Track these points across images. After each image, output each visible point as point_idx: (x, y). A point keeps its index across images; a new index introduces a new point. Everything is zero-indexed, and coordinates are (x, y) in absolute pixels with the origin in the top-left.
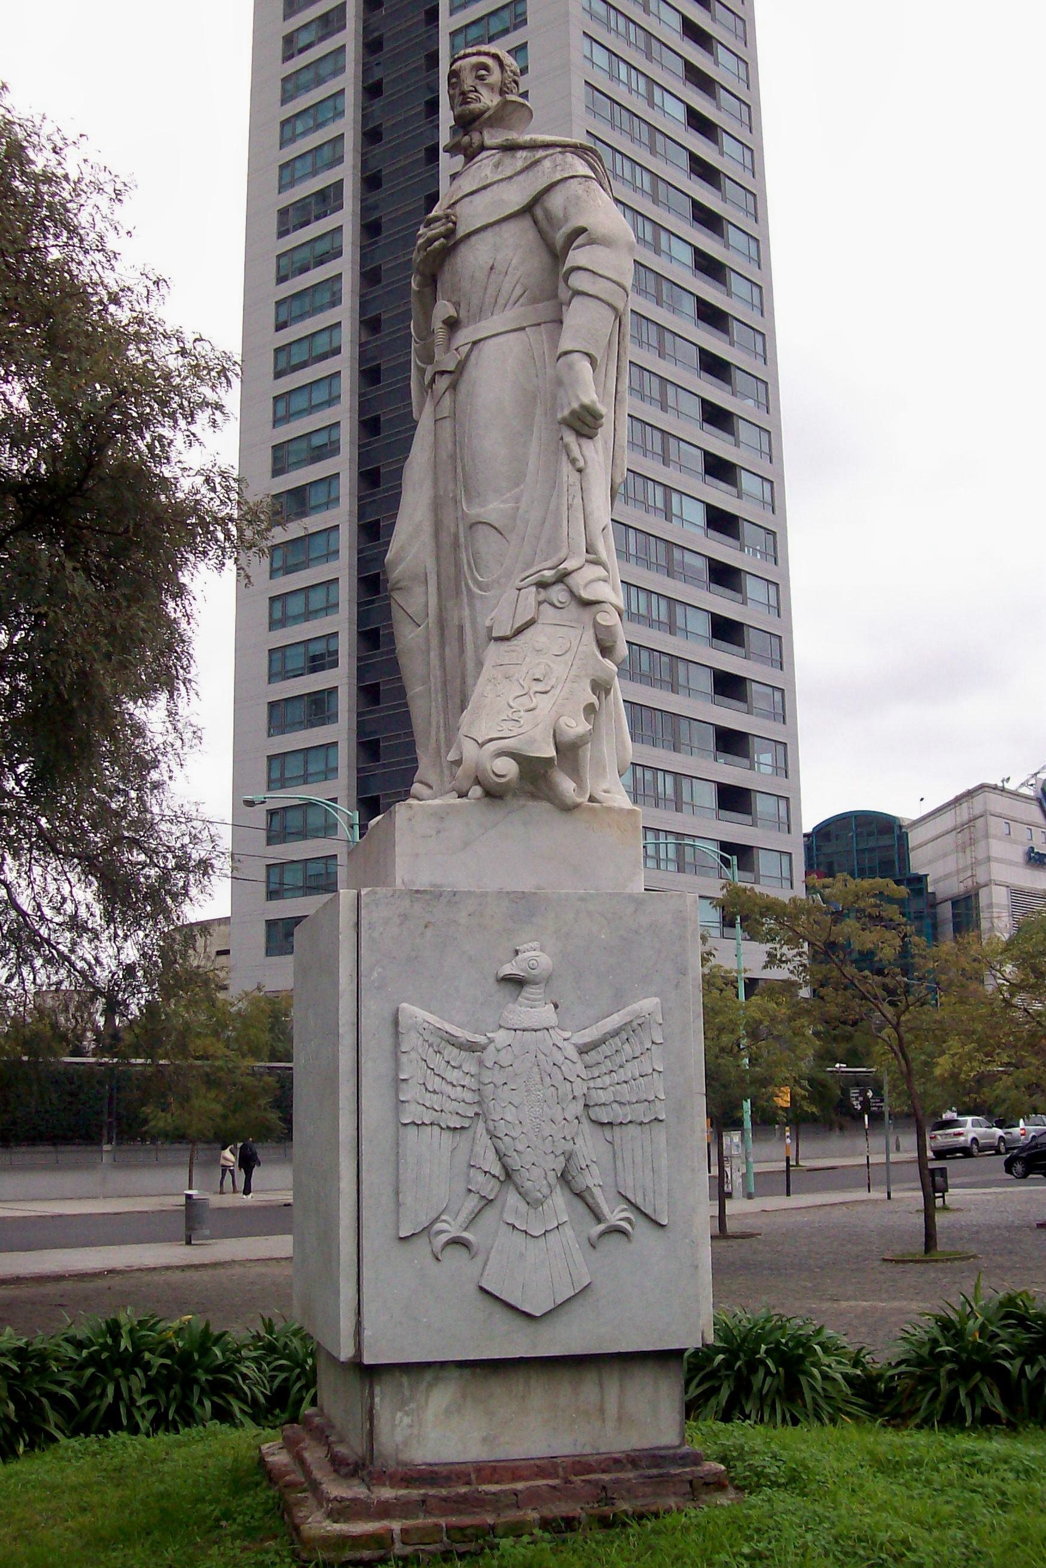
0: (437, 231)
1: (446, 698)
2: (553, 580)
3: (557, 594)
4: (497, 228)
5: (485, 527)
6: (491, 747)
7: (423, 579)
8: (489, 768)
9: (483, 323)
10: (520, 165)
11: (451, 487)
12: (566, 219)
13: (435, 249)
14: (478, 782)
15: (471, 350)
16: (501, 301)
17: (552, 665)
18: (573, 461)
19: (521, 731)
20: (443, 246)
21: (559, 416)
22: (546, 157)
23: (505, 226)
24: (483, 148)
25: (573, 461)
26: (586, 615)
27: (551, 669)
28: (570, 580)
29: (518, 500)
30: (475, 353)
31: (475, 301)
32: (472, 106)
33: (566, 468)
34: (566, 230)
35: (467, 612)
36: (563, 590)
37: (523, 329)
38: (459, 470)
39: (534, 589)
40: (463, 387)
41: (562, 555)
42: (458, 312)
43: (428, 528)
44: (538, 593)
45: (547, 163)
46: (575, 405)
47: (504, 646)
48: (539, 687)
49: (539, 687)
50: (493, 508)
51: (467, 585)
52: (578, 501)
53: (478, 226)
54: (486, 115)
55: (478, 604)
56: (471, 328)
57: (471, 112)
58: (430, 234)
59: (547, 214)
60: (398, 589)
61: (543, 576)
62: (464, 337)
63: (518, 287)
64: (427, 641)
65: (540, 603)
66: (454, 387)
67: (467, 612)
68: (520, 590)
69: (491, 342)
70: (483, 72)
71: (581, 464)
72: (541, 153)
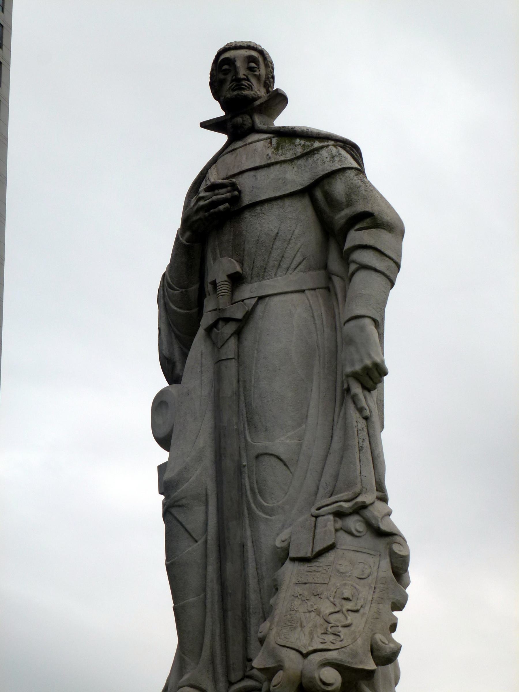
0: (224, 196)
1: (224, 610)
2: (351, 511)
3: (354, 523)
4: (280, 203)
5: (274, 460)
6: (316, 658)
7: (204, 499)
8: (317, 676)
9: (266, 282)
10: (299, 151)
11: (235, 420)
12: (349, 204)
13: (220, 211)
15: (257, 304)
16: (284, 265)
17: (358, 587)
18: (361, 410)
19: (343, 644)
20: (227, 210)
21: (349, 370)
22: (322, 148)
23: (287, 202)
24: (253, 130)
25: (361, 410)
26: (381, 544)
27: (357, 590)
28: (367, 513)
29: (301, 438)
30: (260, 308)
31: (259, 262)
32: (246, 92)
33: (354, 416)
34: (346, 213)
35: (249, 533)
36: (360, 521)
37: (303, 291)
38: (242, 405)
39: (331, 517)
41: (357, 489)
42: (242, 268)
43: (209, 456)
44: (335, 521)
45: (324, 153)
46: (368, 362)
47: (304, 567)
48: (350, 605)
49: (350, 605)
50: (281, 443)
51: (249, 509)
52: (366, 444)
53: (263, 198)
54: (258, 102)
55: (262, 526)
56: (256, 285)
57: (246, 97)
58: (214, 198)
59: (329, 197)
60: (180, 506)
61: (341, 506)
62: (248, 291)
63: (298, 255)
64: (206, 555)
65: (337, 530)
66: (238, 333)
67: (249, 533)
68: (317, 517)
70: (253, 65)
71: (367, 413)
72: (317, 144)
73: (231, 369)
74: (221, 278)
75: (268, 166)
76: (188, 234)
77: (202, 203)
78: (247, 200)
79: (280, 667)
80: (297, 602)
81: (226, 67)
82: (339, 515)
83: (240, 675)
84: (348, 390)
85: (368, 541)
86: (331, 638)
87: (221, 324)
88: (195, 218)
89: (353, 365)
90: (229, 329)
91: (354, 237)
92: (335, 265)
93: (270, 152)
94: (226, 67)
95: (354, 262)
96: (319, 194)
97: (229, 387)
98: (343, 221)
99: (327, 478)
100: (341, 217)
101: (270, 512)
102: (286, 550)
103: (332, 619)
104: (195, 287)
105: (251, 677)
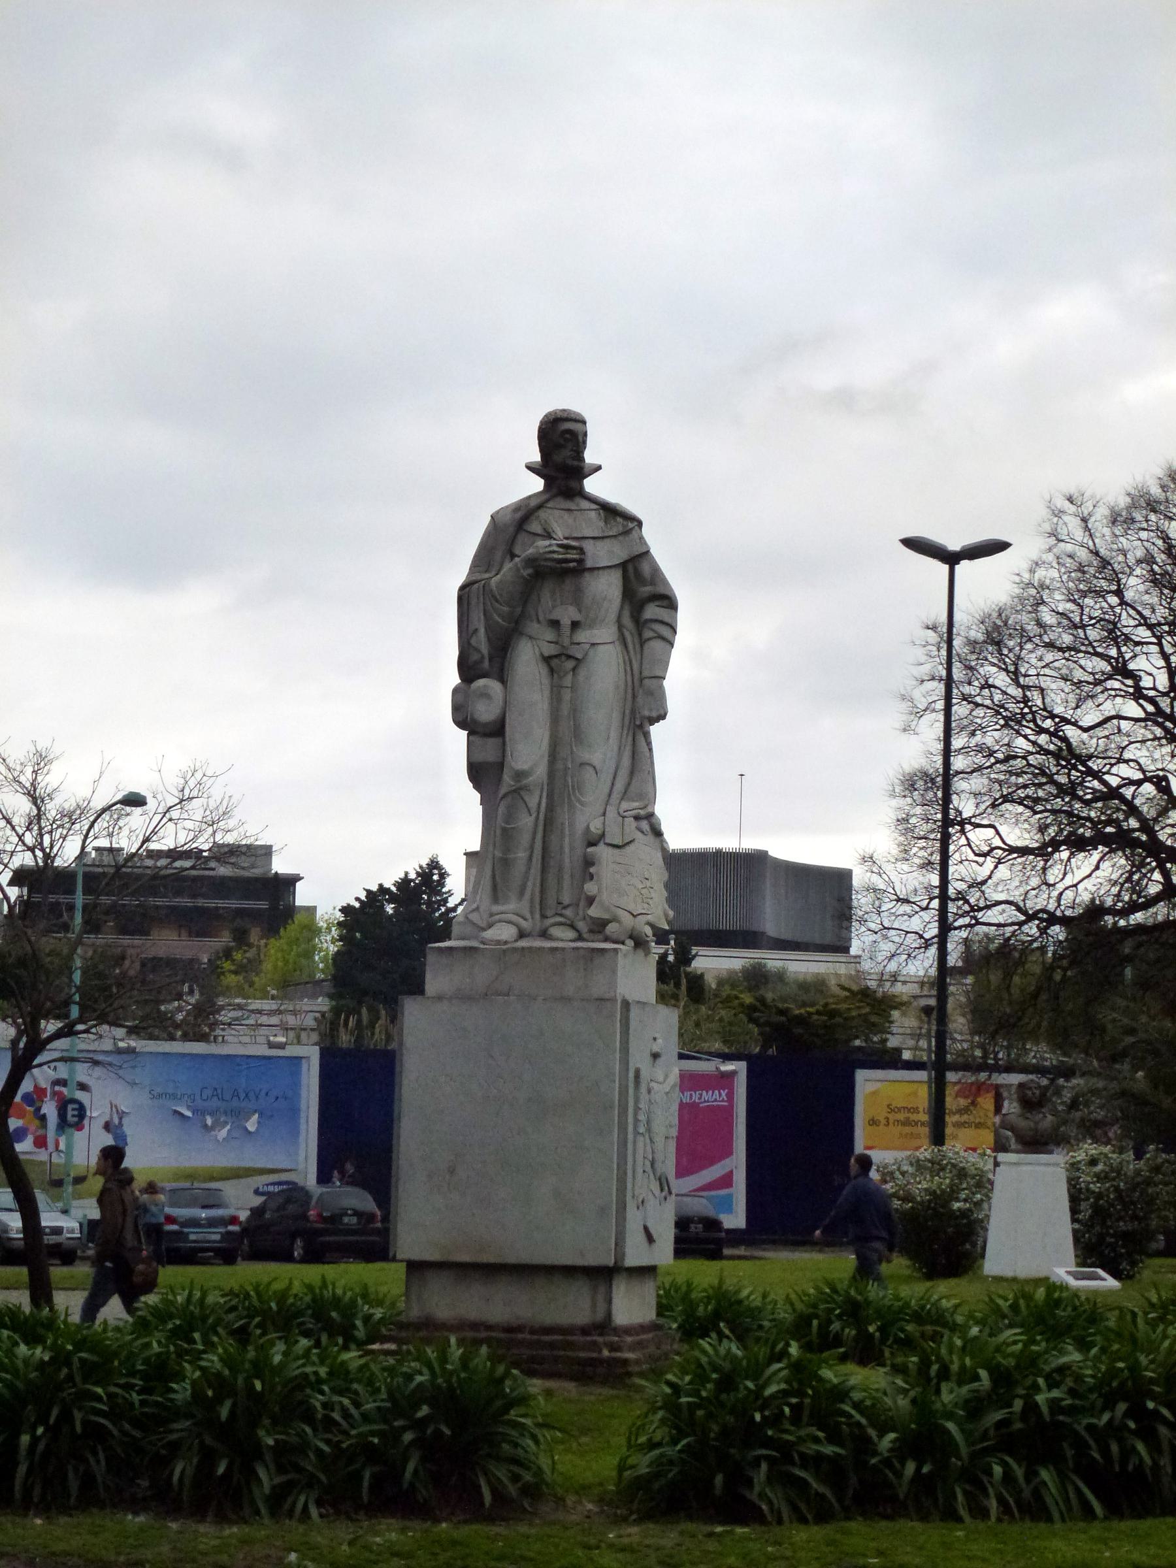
3: (645, 825)
4: (608, 570)
9: (595, 631)
10: (621, 529)
14: (631, 937)
23: (613, 570)
26: (658, 840)
30: (591, 653)
40: (582, 672)
49: (648, 884)
50: (596, 757)
58: (569, 556)
66: (574, 669)
69: (601, 647)
73: (567, 695)
74: (566, 622)
75: (603, 538)
76: (530, 571)
77: (556, 556)
78: (589, 564)
79: (615, 919)
80: (618, 876)
81: (568, 436)
82: (637, 818)
83: (553, 912)
84: (641, 726)
85: (651, 838)
86: (646, 906)
87: (563, 658)
88: (542, 563)
89: (651, 710)
90: (570, 664)
91: (652, 611)
92: (627, 621)
93: (602, 524)
94: (568, 436)
95: (653, 630)
96: (630, 568)
97: (565, 709)
98: (646, 595)
99: (620, 786)
100: (646, 590)
101: (582, 804)
102: (603, 835)
103: (643, 891)
104: (519, 610)
105: (561, 915)
